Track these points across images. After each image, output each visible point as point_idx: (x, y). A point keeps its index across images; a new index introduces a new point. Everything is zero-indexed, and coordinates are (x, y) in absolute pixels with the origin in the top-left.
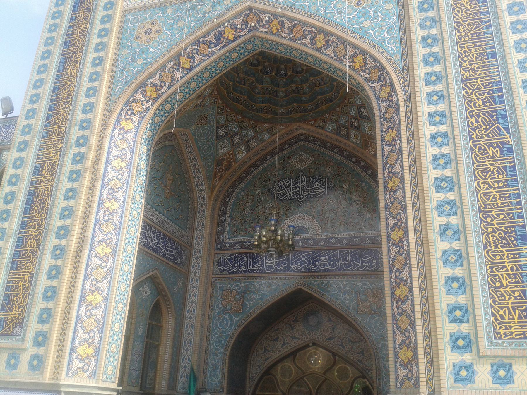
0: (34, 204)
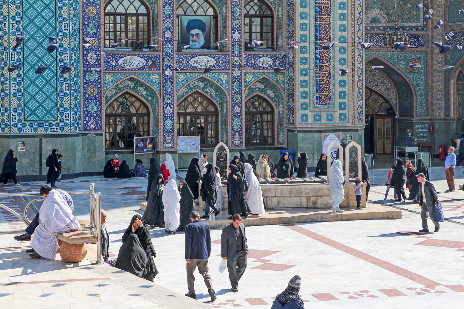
0: (322, 33)
